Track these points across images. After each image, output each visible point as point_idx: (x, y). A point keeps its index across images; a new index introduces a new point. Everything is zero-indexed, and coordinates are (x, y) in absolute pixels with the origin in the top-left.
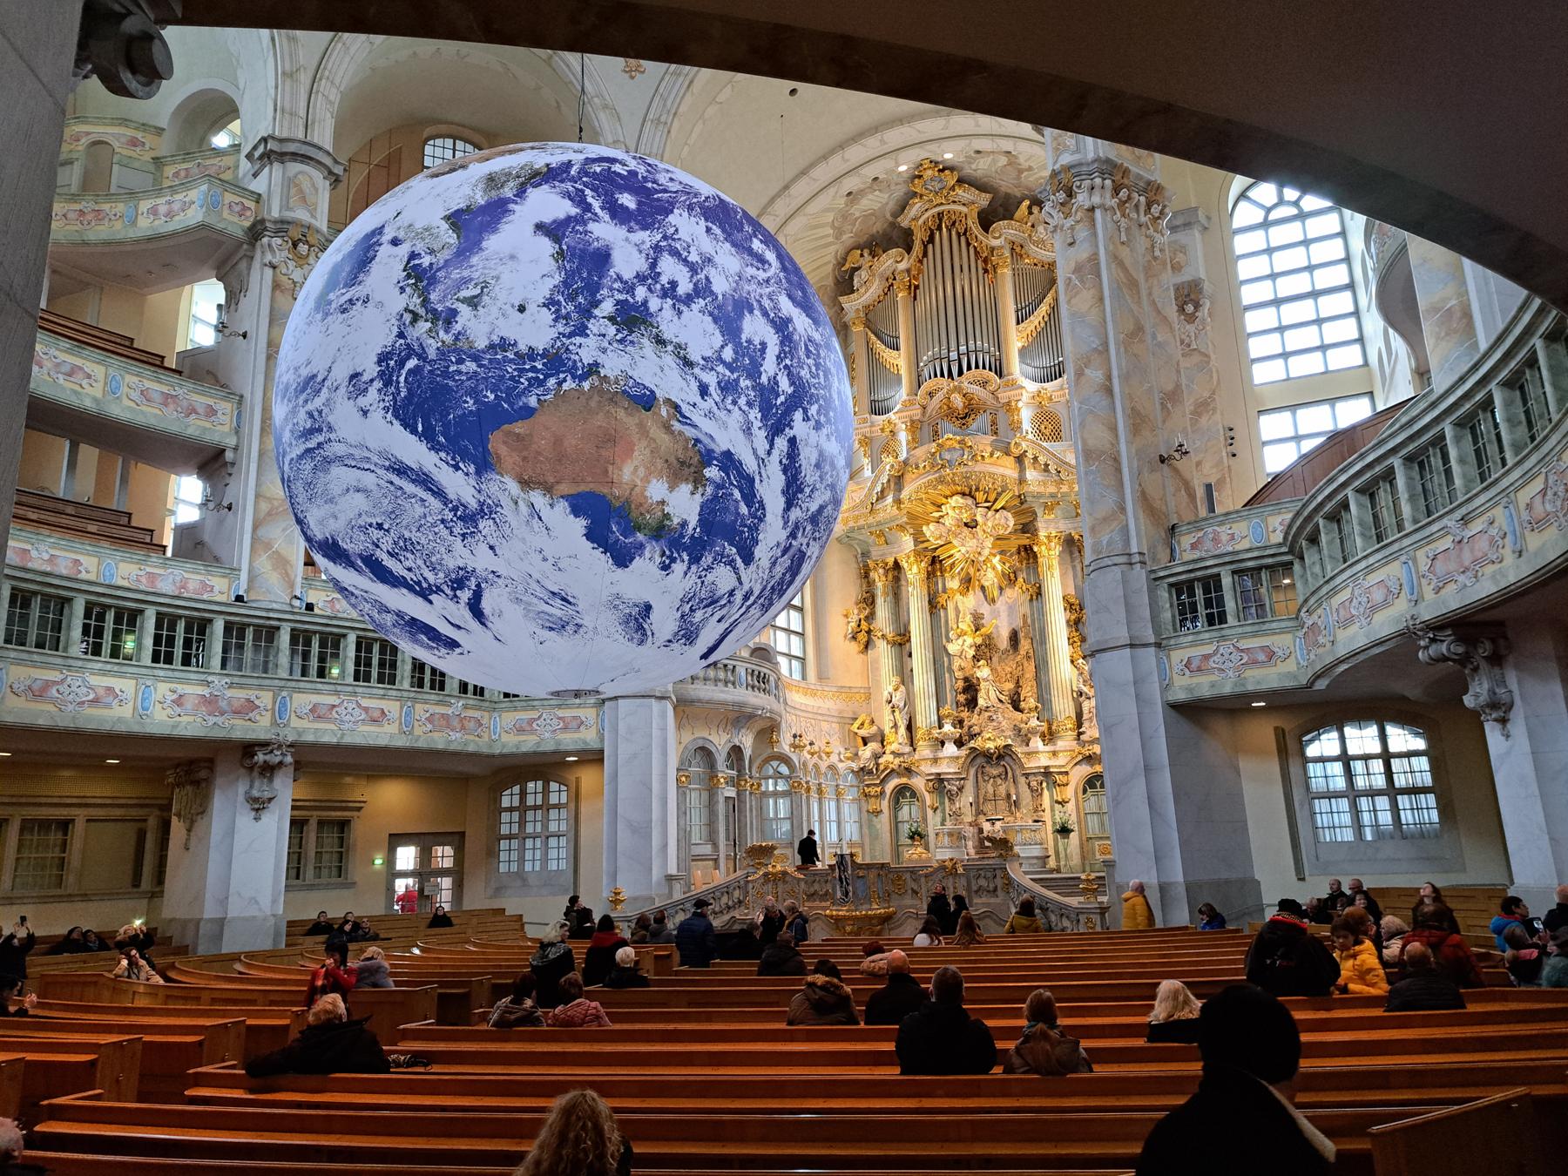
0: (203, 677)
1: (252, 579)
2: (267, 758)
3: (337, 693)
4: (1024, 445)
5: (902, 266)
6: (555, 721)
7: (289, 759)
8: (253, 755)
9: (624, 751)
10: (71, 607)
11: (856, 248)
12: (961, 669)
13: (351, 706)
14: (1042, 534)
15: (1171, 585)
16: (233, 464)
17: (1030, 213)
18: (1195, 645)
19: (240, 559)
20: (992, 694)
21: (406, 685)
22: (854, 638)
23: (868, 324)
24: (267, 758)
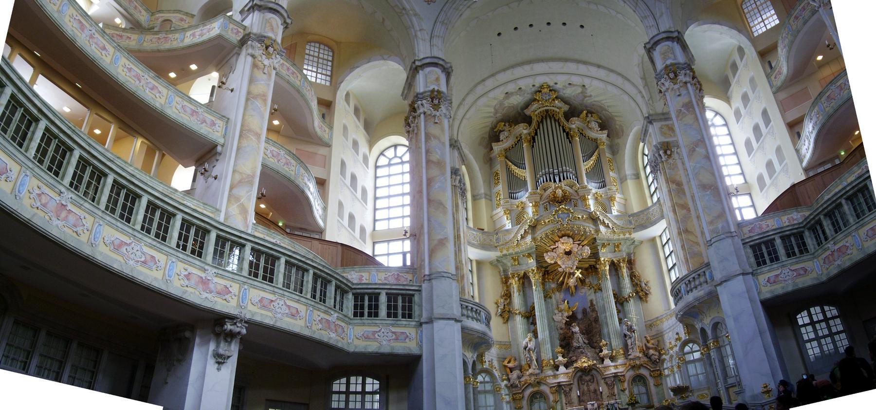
0: (203, 265)
1: (226, 219)
2: (232, 327)
3: (274, 293)
5: (525, 132)
6: (390, 334)
7: (244, 331)
8: (222, 324)
9: (439, 352)
10: (140, 201)
13: (282, 303)
15: (751, 246)
16: (220, 154)
18: (768, 273)
19: (221, 204)
21: (309, 296)
23: (506, 157)
24: (232, 327)
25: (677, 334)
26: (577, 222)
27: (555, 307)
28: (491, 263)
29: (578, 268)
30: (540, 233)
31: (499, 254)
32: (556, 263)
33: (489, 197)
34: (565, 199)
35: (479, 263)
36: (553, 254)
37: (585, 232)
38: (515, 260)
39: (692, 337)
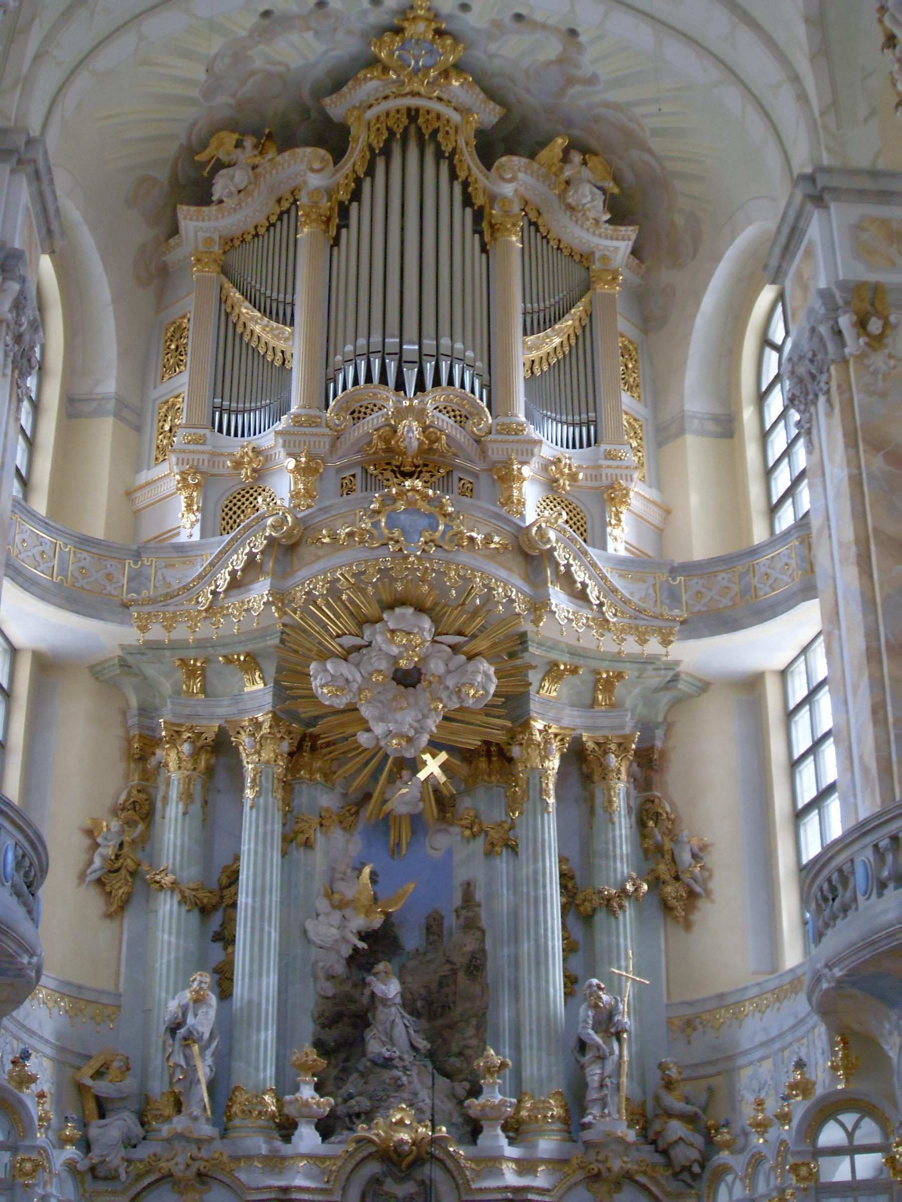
4: (552, 535)
11: (233, 131)
12: (331, 977)
14: (538, 725)
17: (565, 159)
20: (399, 1031)
22: (99, 882)
23: (225, 271)
25: (800, 1065)
26: (464, 557)
27: (319, 883)
28: (96, 671)
29: (435, 746)
30: (310, 577)
31: (131, 635)
32: (352, 709)
33: (131, 415)
34: (431, 463)
35: (47, 666)
36: (346, 669)
37: (488, 599)
38: (191, 673)
39: (861, 1087)
